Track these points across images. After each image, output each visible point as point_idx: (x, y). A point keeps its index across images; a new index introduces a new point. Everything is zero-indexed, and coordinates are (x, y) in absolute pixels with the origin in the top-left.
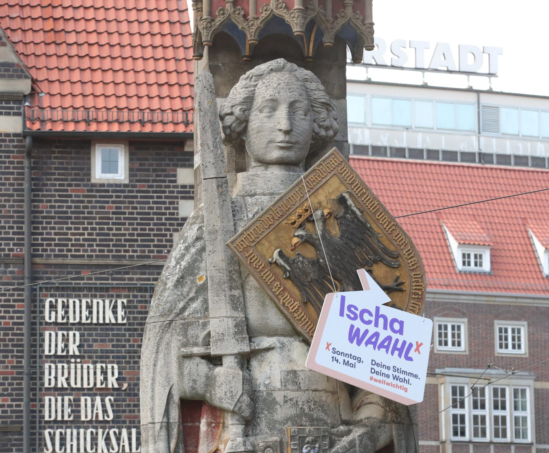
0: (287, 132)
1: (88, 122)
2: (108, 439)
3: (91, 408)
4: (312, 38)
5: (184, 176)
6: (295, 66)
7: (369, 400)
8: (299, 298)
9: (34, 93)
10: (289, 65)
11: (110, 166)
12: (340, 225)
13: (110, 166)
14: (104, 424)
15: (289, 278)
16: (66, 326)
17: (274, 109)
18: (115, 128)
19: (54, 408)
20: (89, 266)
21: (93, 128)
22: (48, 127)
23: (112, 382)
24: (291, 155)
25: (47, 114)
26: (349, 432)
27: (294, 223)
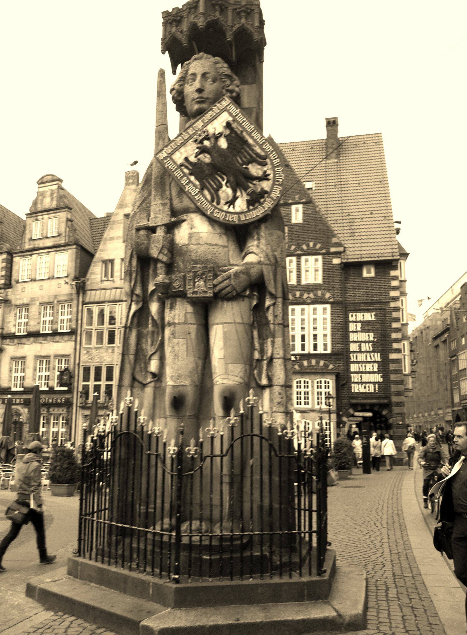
0: (200, 91)
1: (361, 258)
2: (371, 357)
3: (365, 347)
4: (234, 50)
5: (393, 273)
6: (210, 56)
7: (251, 251)
8: (199, 187)
9: (344, 251)
10: (205, 55)
11: (369, 272)
12: (227, 140)
13: (369, 272)
14: (369, 352)
15: (191, 174)
16: (356, 322)
17: (194, 80)
18: (370, 259)
19: (353, 347)
20: (363, 303)
21: (363, 260)
22: (349, 260)
23: (371, 339)
24: (204, 106)
25: (350, 257)
26: (230, 269)
27: (196, 141)
